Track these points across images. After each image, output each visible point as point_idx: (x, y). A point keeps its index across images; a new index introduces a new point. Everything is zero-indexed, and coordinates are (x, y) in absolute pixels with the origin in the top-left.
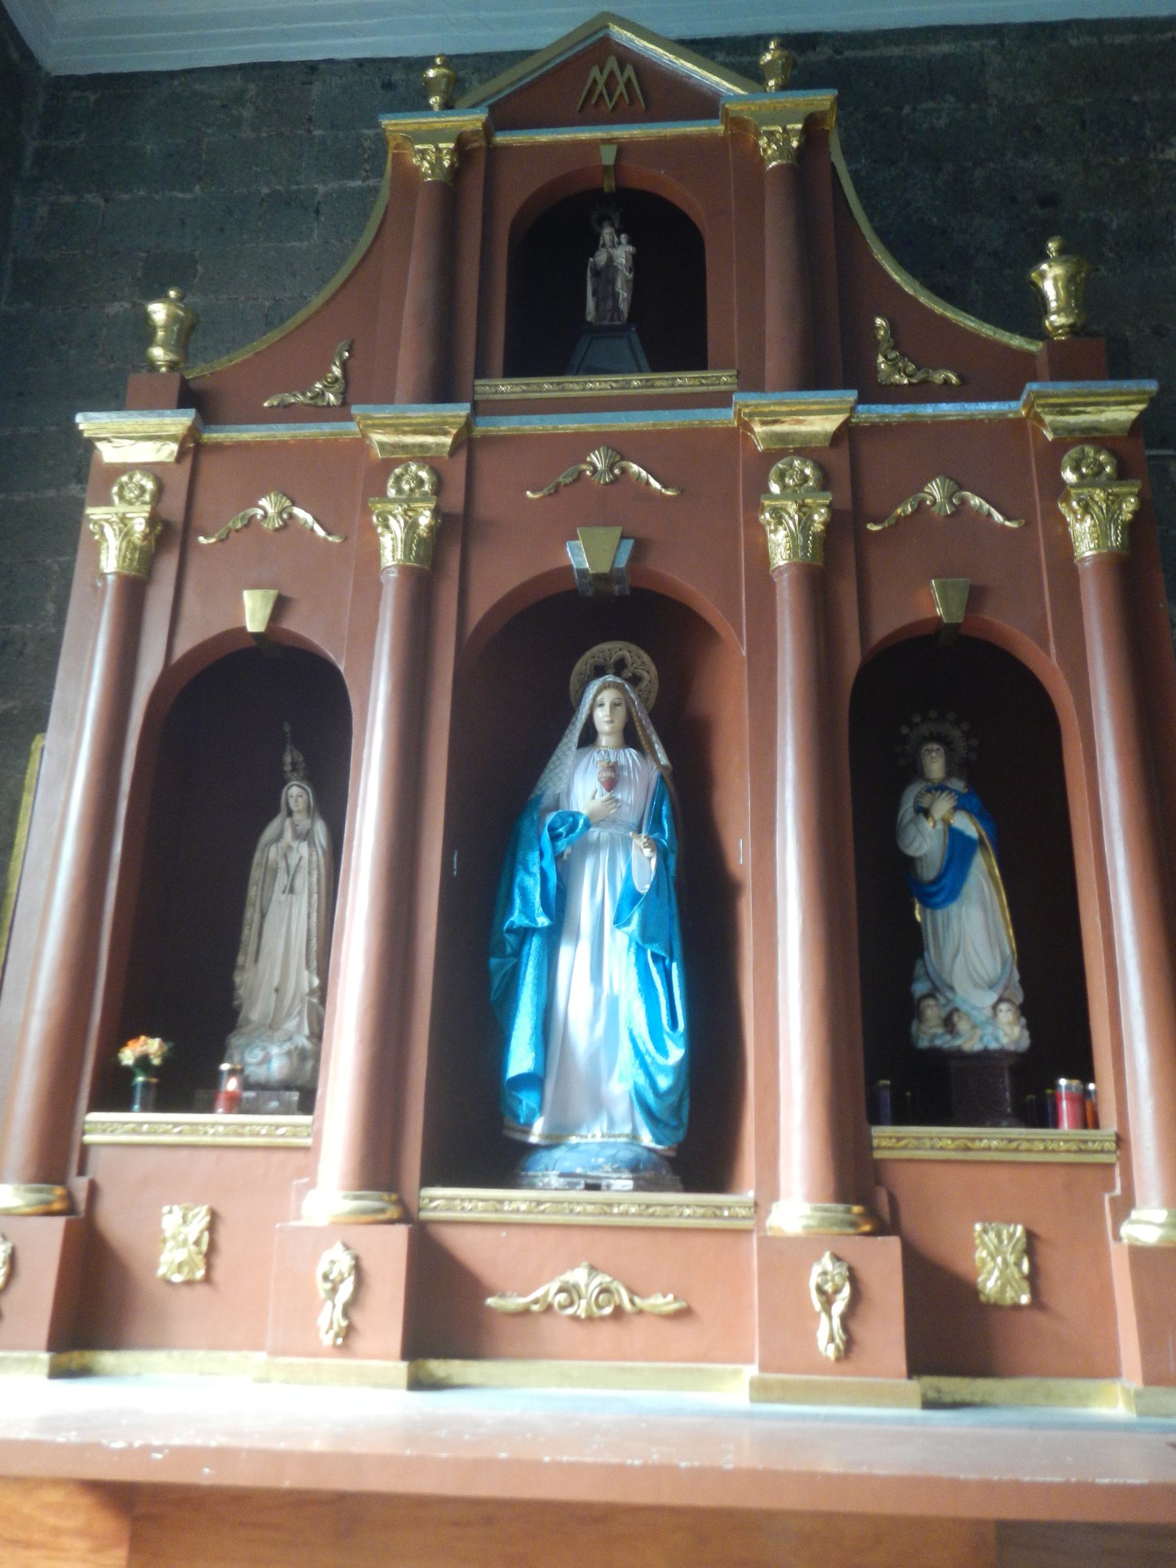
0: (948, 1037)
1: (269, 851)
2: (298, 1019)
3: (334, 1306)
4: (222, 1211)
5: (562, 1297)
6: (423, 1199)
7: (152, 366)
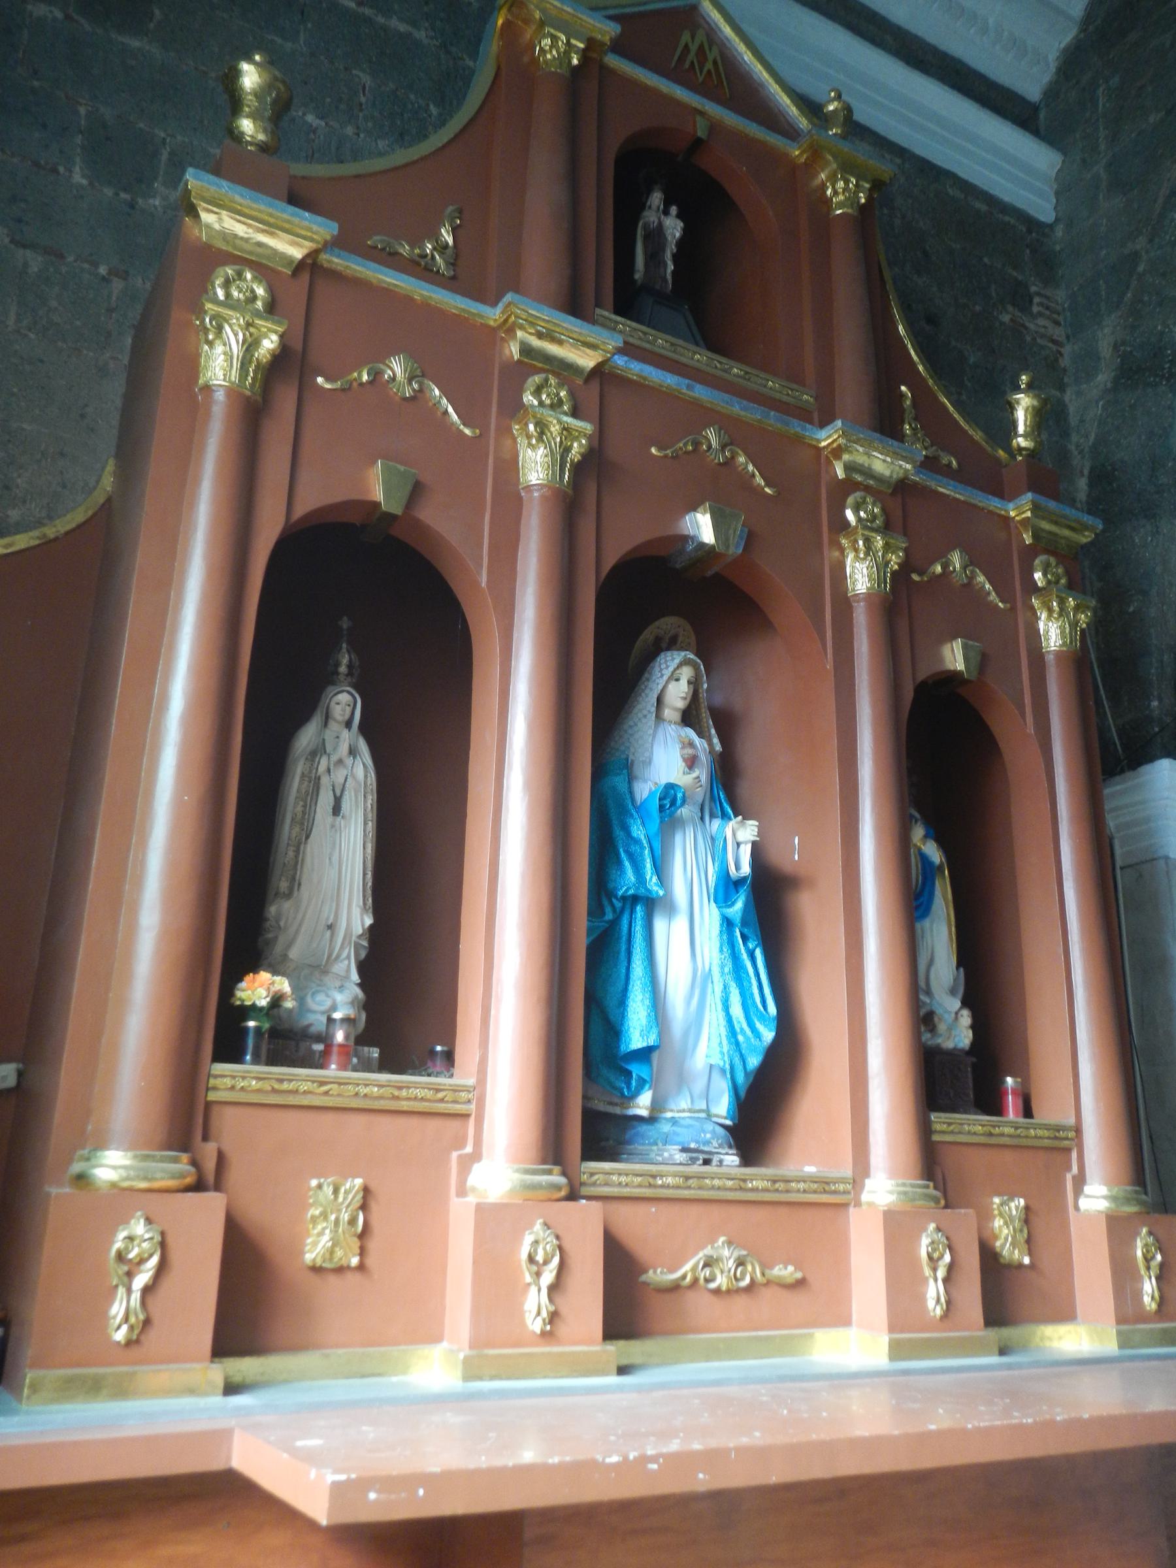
0: (929, 1035)
1: (319, 763)
2: (346, 962)
3: (539, 1290)
4: (373, 1186)
5: (707, 1271)
6: (584, 1173)
7: (236, 136)
